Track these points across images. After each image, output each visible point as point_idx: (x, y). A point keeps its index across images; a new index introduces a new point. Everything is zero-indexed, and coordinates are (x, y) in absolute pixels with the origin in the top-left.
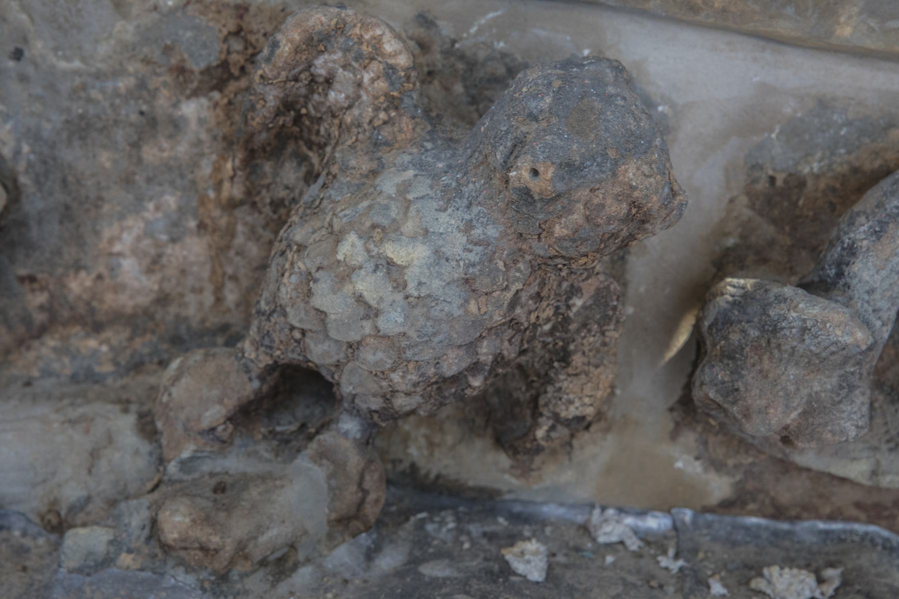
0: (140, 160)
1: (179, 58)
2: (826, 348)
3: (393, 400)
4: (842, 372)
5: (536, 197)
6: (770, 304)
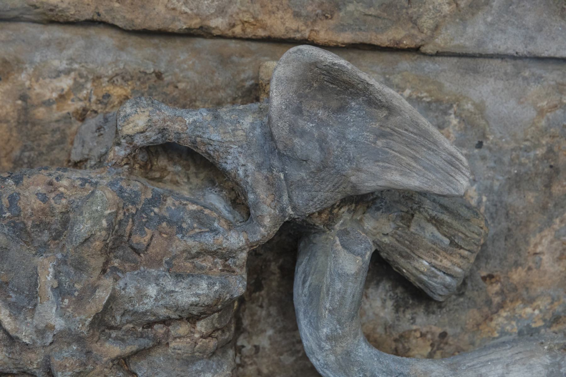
0: (551, 194)
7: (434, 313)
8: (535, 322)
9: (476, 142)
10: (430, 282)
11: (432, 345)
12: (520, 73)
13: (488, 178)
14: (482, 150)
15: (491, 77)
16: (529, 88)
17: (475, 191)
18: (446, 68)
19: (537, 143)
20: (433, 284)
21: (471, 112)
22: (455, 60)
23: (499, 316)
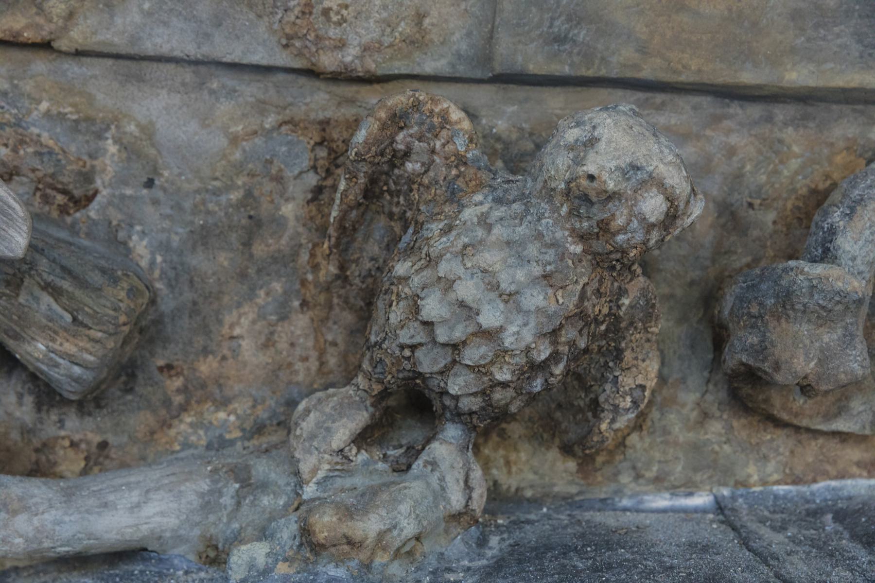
0: (251, 256)
1: (277, 169)
2: (830, 300)
3: (492, 396)
4: (844, 324)
5: (594, 199)
6: (780, 277)
7: (90, 414)
8: (230, 432)
9: (145, 180)
10: (52, 373)
11: (87, 459)
12: (204, 83)
13: (163, 230)
14: (153, 190)
15: (163, 88)
16: (218, 105)
17: (146, 247)
18: (98, 73)
19: (229, 183)
20: (56, 375)
21: (136, 137)
22: (110, 62)
23: (181, 421)
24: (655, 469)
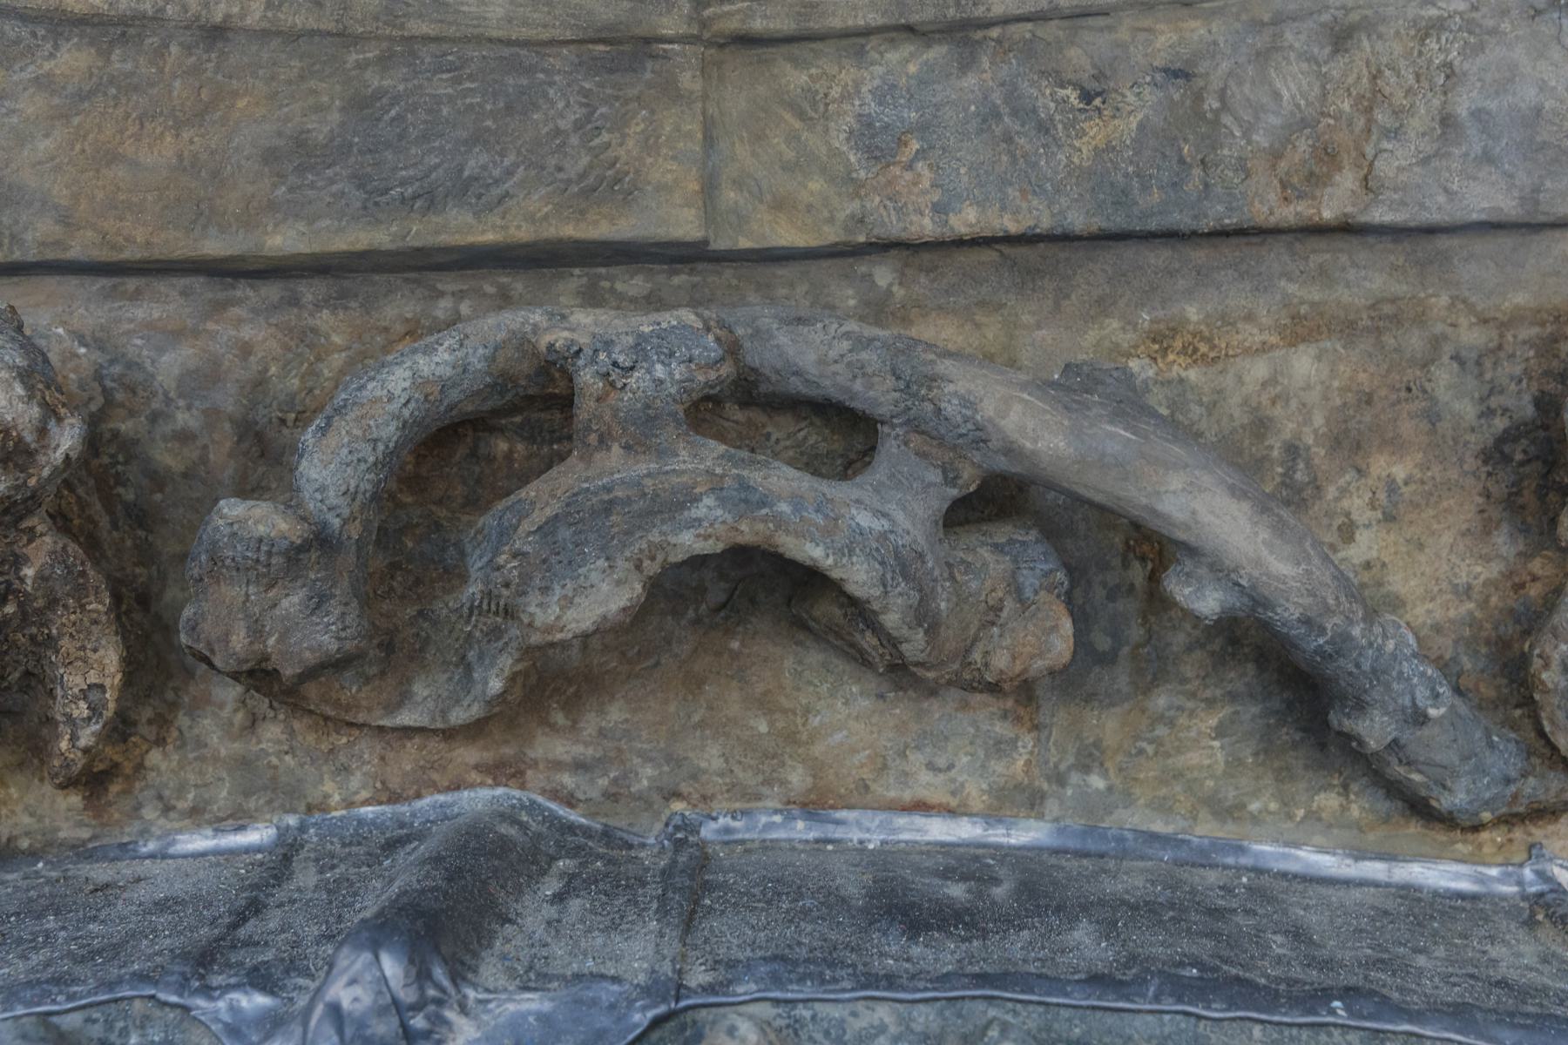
24: (191, 796)
